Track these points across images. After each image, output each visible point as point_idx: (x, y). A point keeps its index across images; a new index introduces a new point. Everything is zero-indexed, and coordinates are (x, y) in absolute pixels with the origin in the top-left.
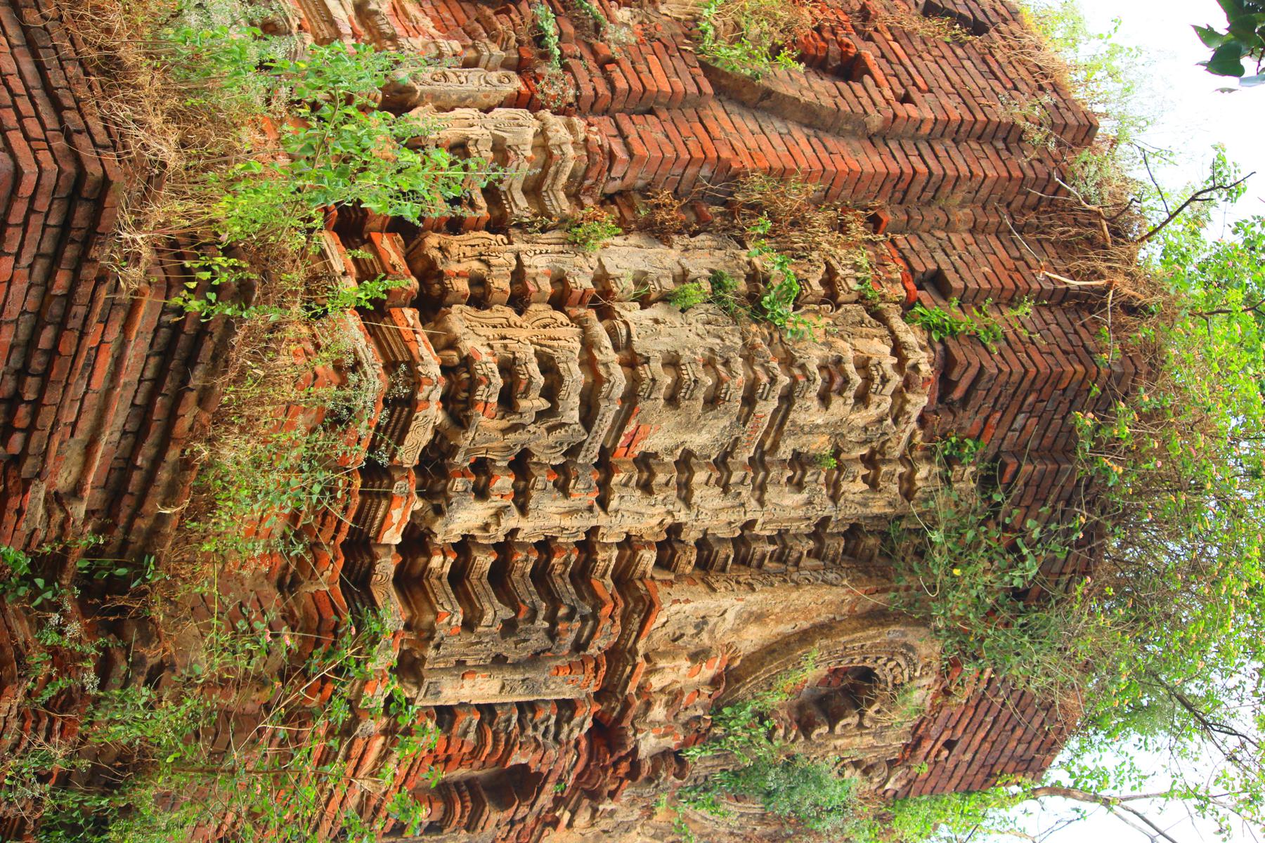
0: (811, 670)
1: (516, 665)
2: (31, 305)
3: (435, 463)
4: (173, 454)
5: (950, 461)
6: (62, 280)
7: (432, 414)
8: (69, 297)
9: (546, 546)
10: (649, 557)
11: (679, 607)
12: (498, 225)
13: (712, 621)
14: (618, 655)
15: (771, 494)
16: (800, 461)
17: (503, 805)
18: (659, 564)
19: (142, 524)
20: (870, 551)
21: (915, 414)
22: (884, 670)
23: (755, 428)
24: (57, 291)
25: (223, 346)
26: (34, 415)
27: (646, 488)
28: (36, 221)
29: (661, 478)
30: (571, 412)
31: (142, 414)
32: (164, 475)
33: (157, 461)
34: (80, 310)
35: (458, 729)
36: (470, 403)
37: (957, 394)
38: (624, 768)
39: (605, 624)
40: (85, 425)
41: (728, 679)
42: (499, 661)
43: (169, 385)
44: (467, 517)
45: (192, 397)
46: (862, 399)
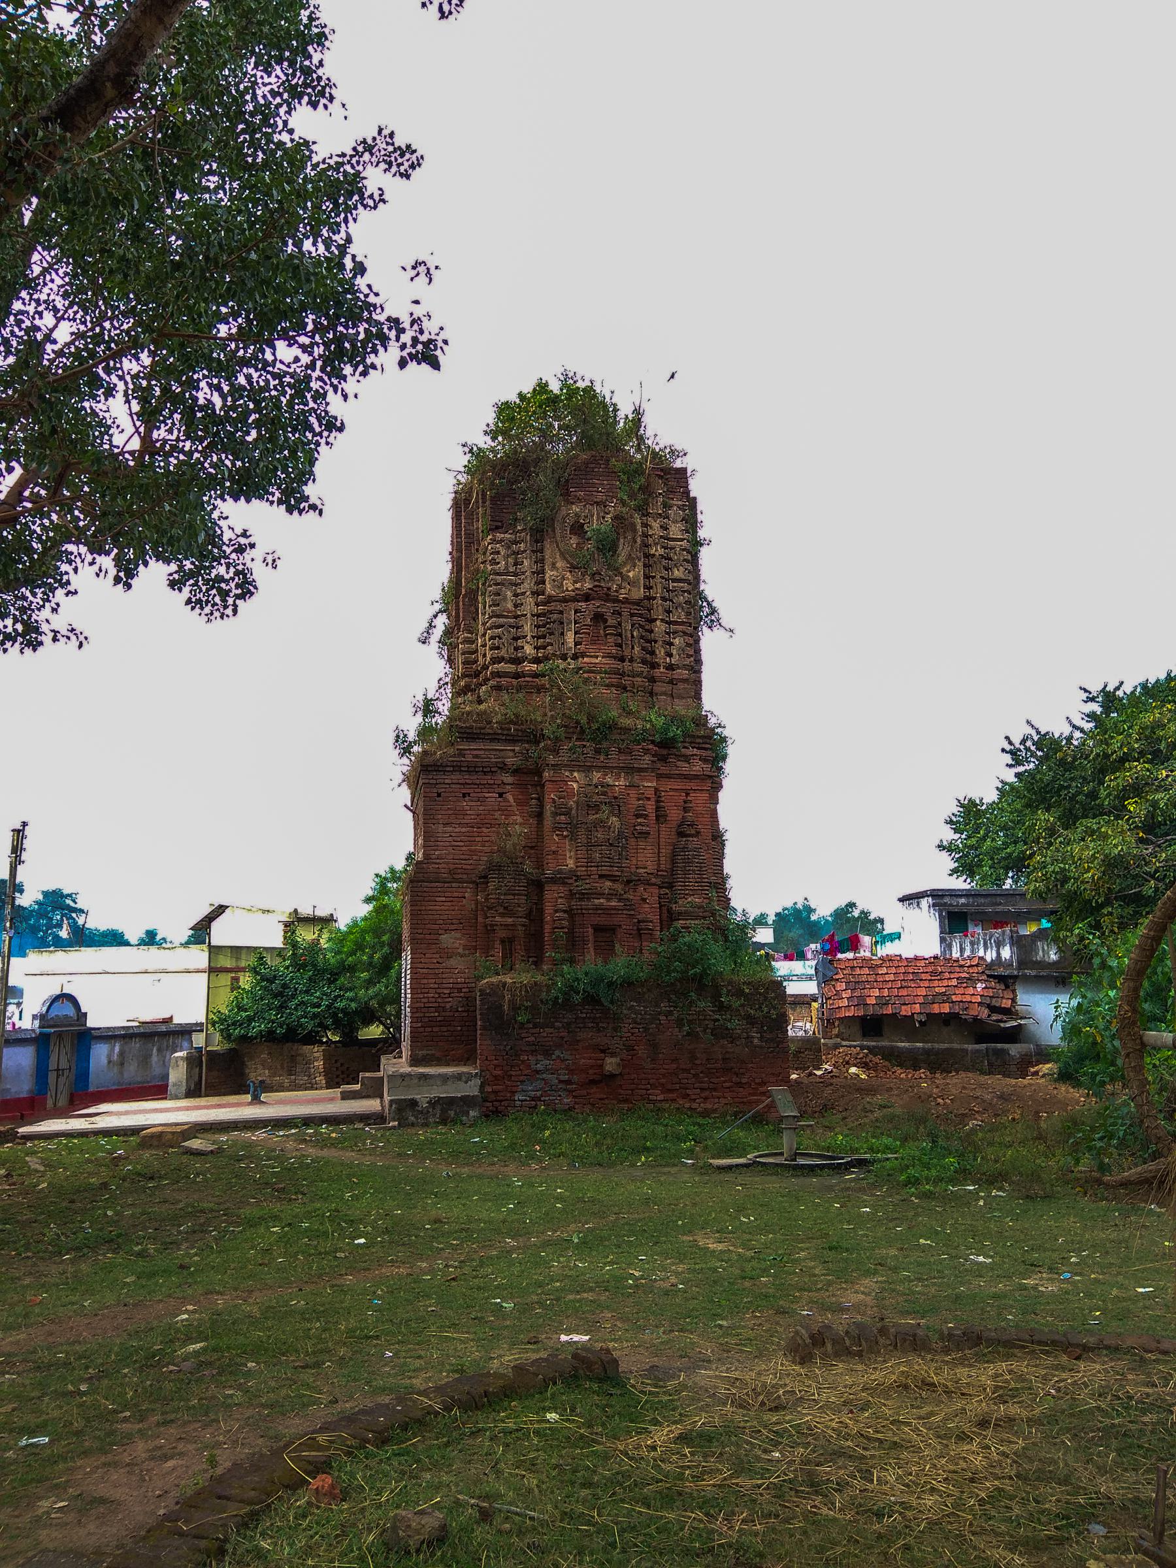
0: (574, 541)
3: (517, 661)
5: (516, 519)
7: (502, 667)
9: (538, 626)
11: (549, 589)
12: (476, 651)
14: (565, 600)
17: (606, 621)
20: (539, 535)
31: (492, 740)
41: (573, 568)
42: (562, 634)
44: (529, 650)
46: (498, 553)
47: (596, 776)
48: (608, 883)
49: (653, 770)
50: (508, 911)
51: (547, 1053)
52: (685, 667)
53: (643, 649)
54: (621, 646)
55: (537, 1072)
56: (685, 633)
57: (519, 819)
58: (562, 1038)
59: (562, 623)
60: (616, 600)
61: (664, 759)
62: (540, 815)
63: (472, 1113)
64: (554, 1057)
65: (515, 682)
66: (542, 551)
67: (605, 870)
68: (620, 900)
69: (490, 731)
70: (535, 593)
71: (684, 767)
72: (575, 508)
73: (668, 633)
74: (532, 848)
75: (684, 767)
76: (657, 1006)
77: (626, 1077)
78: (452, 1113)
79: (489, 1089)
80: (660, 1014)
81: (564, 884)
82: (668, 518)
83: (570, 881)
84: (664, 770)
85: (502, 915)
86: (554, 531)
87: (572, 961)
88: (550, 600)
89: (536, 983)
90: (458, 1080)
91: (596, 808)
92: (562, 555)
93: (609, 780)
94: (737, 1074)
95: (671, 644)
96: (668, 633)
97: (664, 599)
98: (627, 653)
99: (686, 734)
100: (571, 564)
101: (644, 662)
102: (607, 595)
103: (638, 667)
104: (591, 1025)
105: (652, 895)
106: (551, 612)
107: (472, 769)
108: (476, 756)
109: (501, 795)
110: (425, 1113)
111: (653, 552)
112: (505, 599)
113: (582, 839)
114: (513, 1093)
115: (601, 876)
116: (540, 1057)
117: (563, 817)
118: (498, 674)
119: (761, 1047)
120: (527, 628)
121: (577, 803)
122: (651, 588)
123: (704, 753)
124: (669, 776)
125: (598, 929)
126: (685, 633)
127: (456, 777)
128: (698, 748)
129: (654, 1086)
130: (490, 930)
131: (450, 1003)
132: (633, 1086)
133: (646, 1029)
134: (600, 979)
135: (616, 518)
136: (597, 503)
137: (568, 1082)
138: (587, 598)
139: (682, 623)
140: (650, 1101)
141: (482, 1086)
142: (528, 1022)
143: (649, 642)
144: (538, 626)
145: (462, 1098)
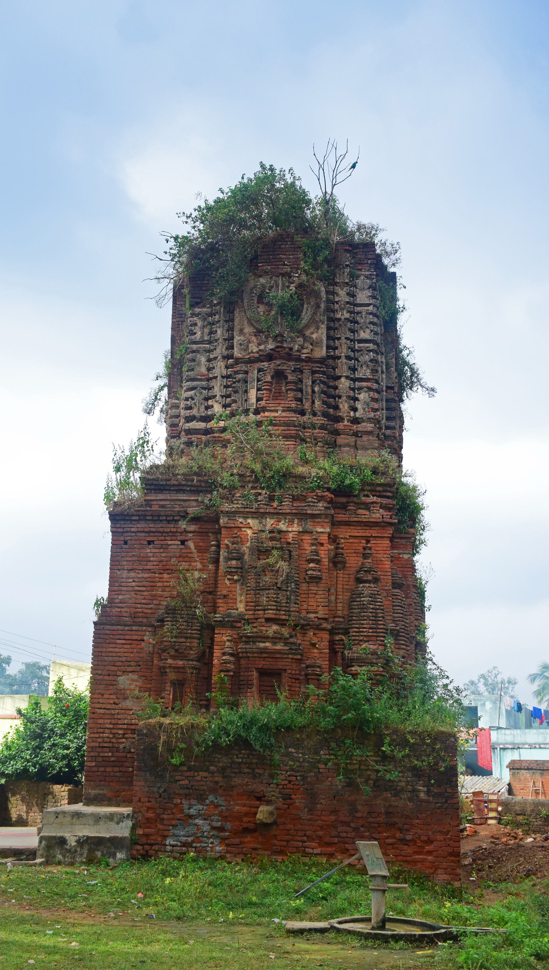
0: (262, 309)
1: (247, 387)
2: (143, 522)
4: (184, 483)
6: (134, 518)
8: (139, 516)
9: (226, 387)
10: (231, 361)
11: (237, 353)
13: (240, 342)
14: (251, 361)
15: (216, 338)
16: (211, 333)
17: (286, 377)
18: (233, 358)
19: (203, 484)
21: (200, 310)
22: (257, 291)
23: (200, 347)
24: (138, 518)
25: (153, 479)
26: (169, 516)
27: (214, 368)
28: (122, 526)
29: (211, 366)
30: (192, 392)
31: (178, 491)
32: (189, 483)
33: (188, 486)
34: (140, 513)
35: (261, 396)
36: (190, 416)
37: (199, 300)
38: (279, 350)
39: (238, 369)
40: (179, 503)
42: (246, 391)
43: (168, 488)
44: (217, 408)
45: (168, 483)
46: (196, 324)
47: (270, 523)
48: (275, 627)
49: (326, 516)
50: (179, 654)
51: (201, 799)
52: (369, 420)
53: (324, 403)
54: (301, 400)
55: (191, 817)
56: (370, 389)
57: (199, 566)
58: (217, 783)
59: (246, 382)
60: (299, 359)
61: (344, 507)
62: (216, 561)
63: (119, 855)
64: (207, 802)
65: (204, 438)
66: (232, 320)
67: (270, 614)
68: (286, 644)
69: (175, 483)
70: (226, 357)
71: (364, 515)
72: (262, 280)
73: (353, 389)
74: (210, 593)
75: (364, 515)
76: (317, 753)
77: (281, 827)
78: (99, 854)
79: (140, 831)
80: (319, 762)
81: (233, 627)
82: (355, 286)
83: (239, 625)
84: (342, 517)
85: (174, 657)
86: (242, 302)
87: (234, 705)
88: (238, 361)
89: (192, 725)
90: (113, 820)
91: (267, 552)
92: (249, 321)
93: (282, 526)
94: (401, 830)
95: (356, 399)
96: (353, 389)
97: (348, 358)
98: (307, 405)
99: (364, 483)
100: (257, 329)
101: (325, 414)
102: (289, 355)
103: (319, 420)
104: (246, 770)
105: (322, 641)
106: (236, 373)
107: (156, 518)
108: (163, 506)
109: (183, 542)
110: (72, 852)
111: (339, 316)
112: (199, 364)
113: (252, 583)
114: (165, 837)
115: (268, 620)
116: (193, 802)
117: (234, 562)
118: (189, 432)
119: (427, 802)
120: (217, 390)
121: (250, 549)
122: (336, 348)
123: (385, 501)
124: (348, 524)
125: (263, 673)
126: (370, 389)
127: (142, 525)
128: (377, 496)
129: (310, 838)
130: (162, 671)
131: (124, 743)
132: (288, 837)
133: (304, 778)
134: (253, 722)
135: (300, 286)
136: (283, 275)
137: (221, 829)
138: (269, 357)
139: (367, 380)
140: (305, 854)
141: (133, 828)
142: (182, 764)
143: (334, 397)
144: (226, 387)
145: (113, 840)
